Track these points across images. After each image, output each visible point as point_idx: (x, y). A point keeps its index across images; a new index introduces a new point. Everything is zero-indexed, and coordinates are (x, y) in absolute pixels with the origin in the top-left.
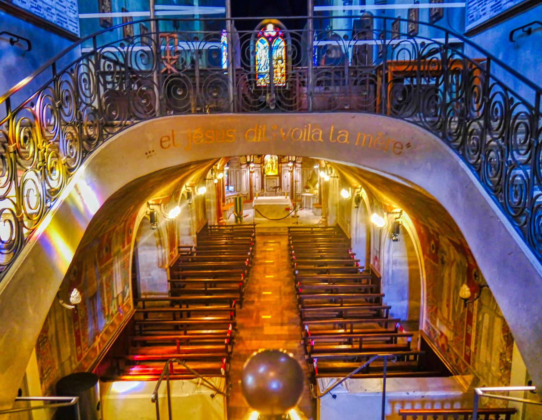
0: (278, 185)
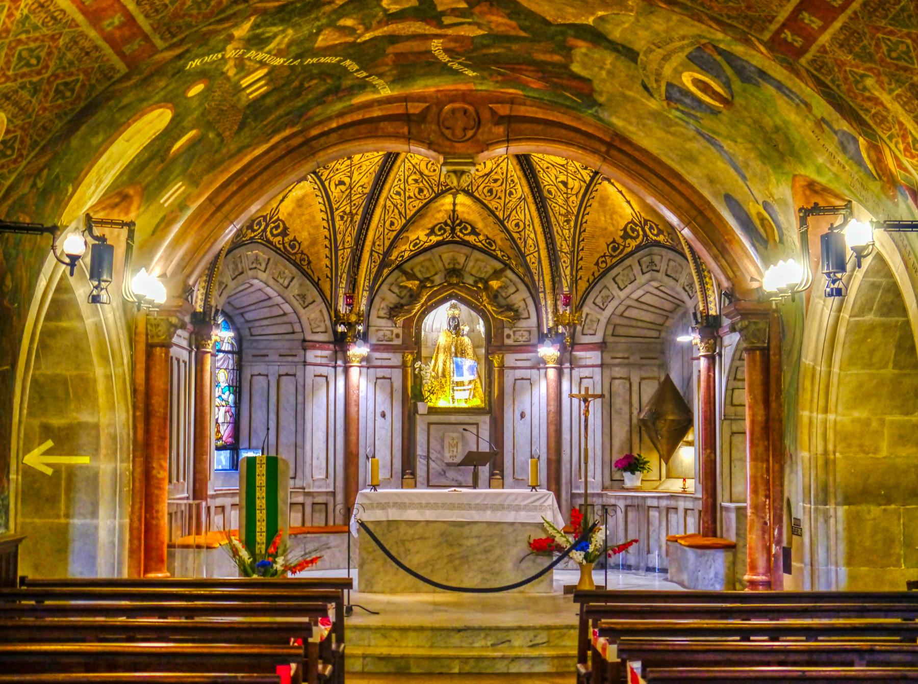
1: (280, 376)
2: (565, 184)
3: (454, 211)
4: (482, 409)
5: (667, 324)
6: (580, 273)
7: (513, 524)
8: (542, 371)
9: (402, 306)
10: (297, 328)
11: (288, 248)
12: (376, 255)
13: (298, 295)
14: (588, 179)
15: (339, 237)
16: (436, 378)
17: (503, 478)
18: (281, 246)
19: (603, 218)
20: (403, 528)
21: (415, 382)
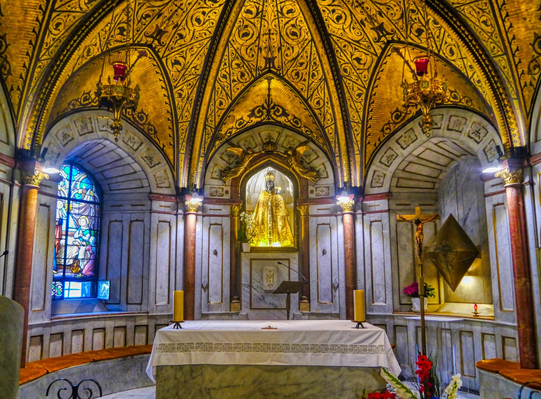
0: (295, 277)
1: (131, 221)
2: (358, 60)
3: (269, 95)
4: (292, 248)
5: (441, 177)
6: (368, 139)
7: (337, 368)
8: (339, 218)
9: (230, 169)
10: (146, 184)
11: (137, 119)
12: (209, 128)
13: (146, 157)
14: (379, 51)
15: (179, 112)
16: (257, 225)
17: (309, 302)
18: (131, 117)
19: (389, 91)
20: (208, 374)
21: (241, 228)
